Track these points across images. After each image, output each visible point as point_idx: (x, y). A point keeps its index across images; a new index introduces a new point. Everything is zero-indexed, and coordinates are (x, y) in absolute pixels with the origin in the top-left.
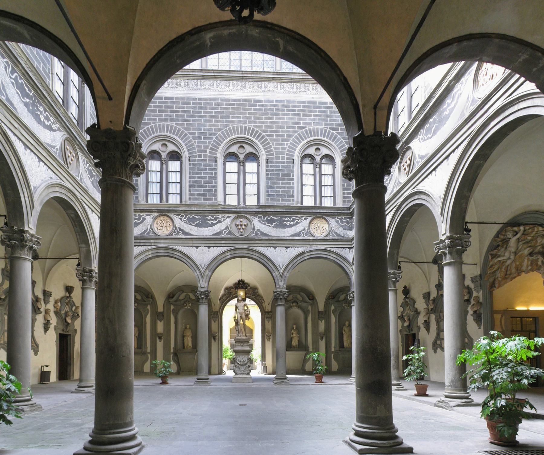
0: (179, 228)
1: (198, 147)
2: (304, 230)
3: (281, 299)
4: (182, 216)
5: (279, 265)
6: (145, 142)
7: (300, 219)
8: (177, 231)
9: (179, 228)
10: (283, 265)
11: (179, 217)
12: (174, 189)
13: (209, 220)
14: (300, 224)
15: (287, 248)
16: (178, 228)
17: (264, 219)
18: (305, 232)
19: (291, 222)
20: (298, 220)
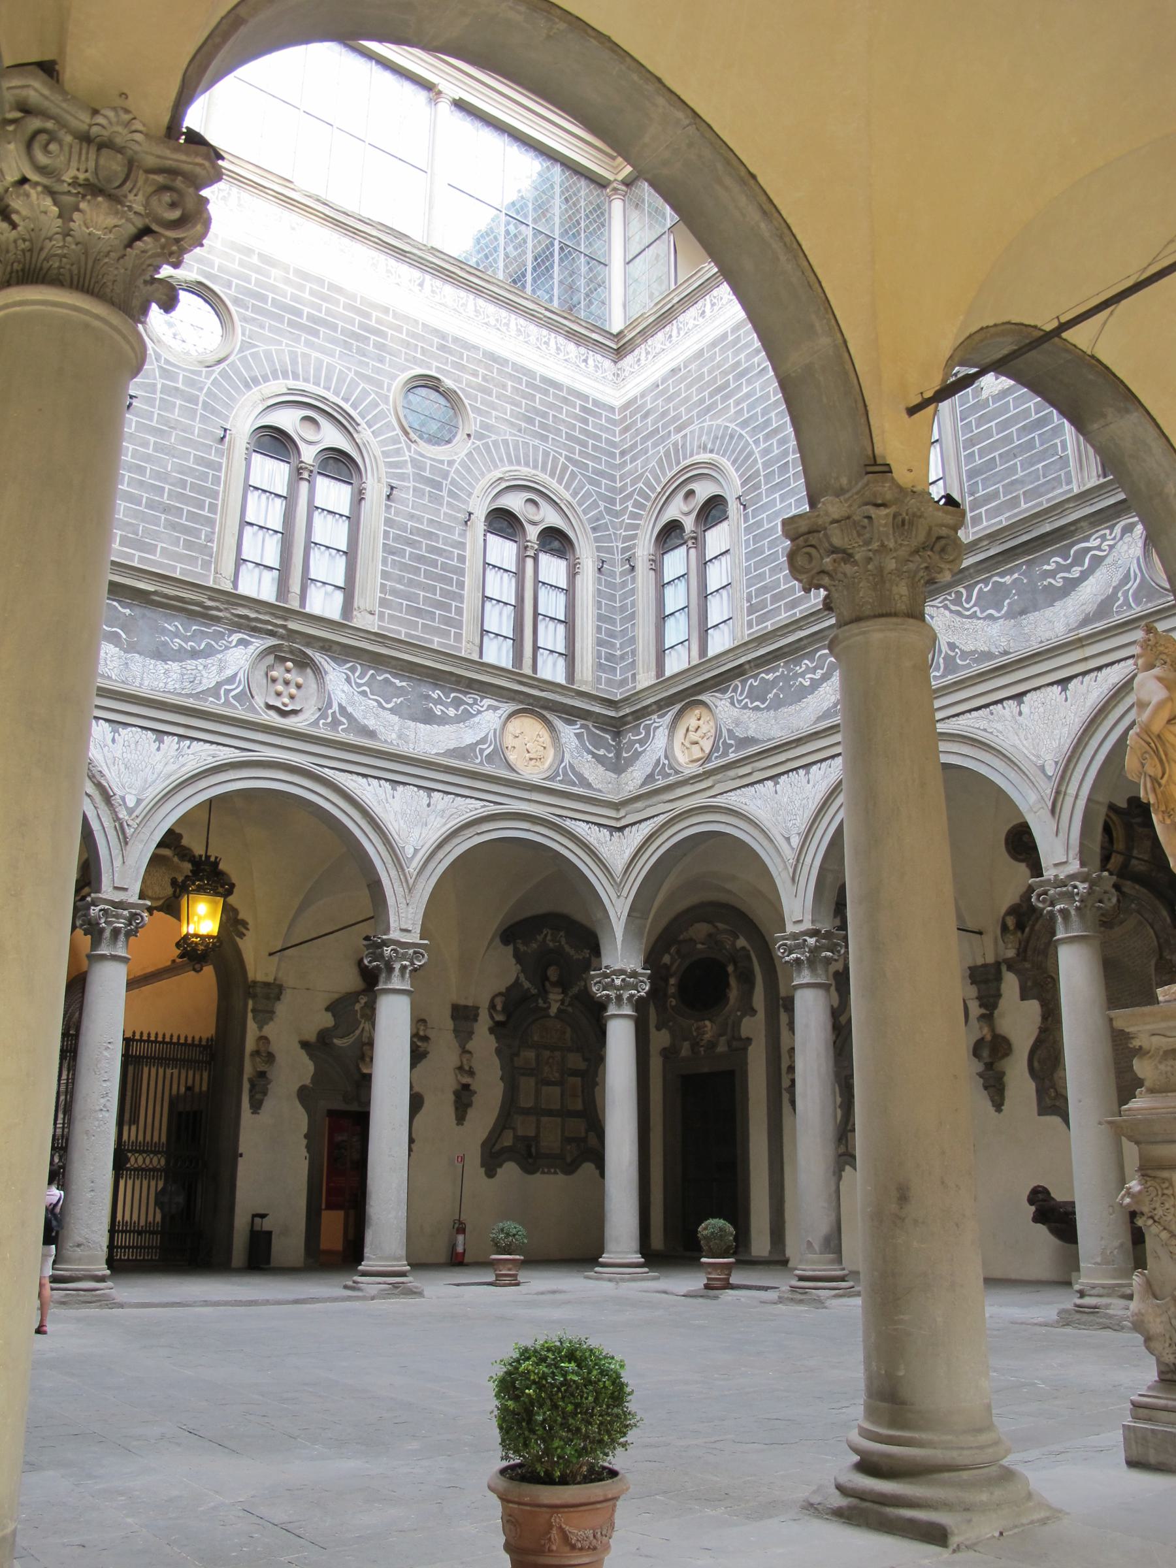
0: (728, 730)
1: (766, 451)
2: (1126, 578)
3: (1065, 913)
4: (735, 690)
5: (1042, 769)
6: (647, 509)
7: (1104, 538)
8: (724, 743)
9: (728, 730)
10: (1056, 763)
11: (728, 695)
12: (717, 610)
13: (803, 675)
14: (1109, 560)
15: (1064, 682)
16: (725, 733)
17: (968, 600)
18: (1132, 586)
19: (1068, 568)
20: (1099, 548)
